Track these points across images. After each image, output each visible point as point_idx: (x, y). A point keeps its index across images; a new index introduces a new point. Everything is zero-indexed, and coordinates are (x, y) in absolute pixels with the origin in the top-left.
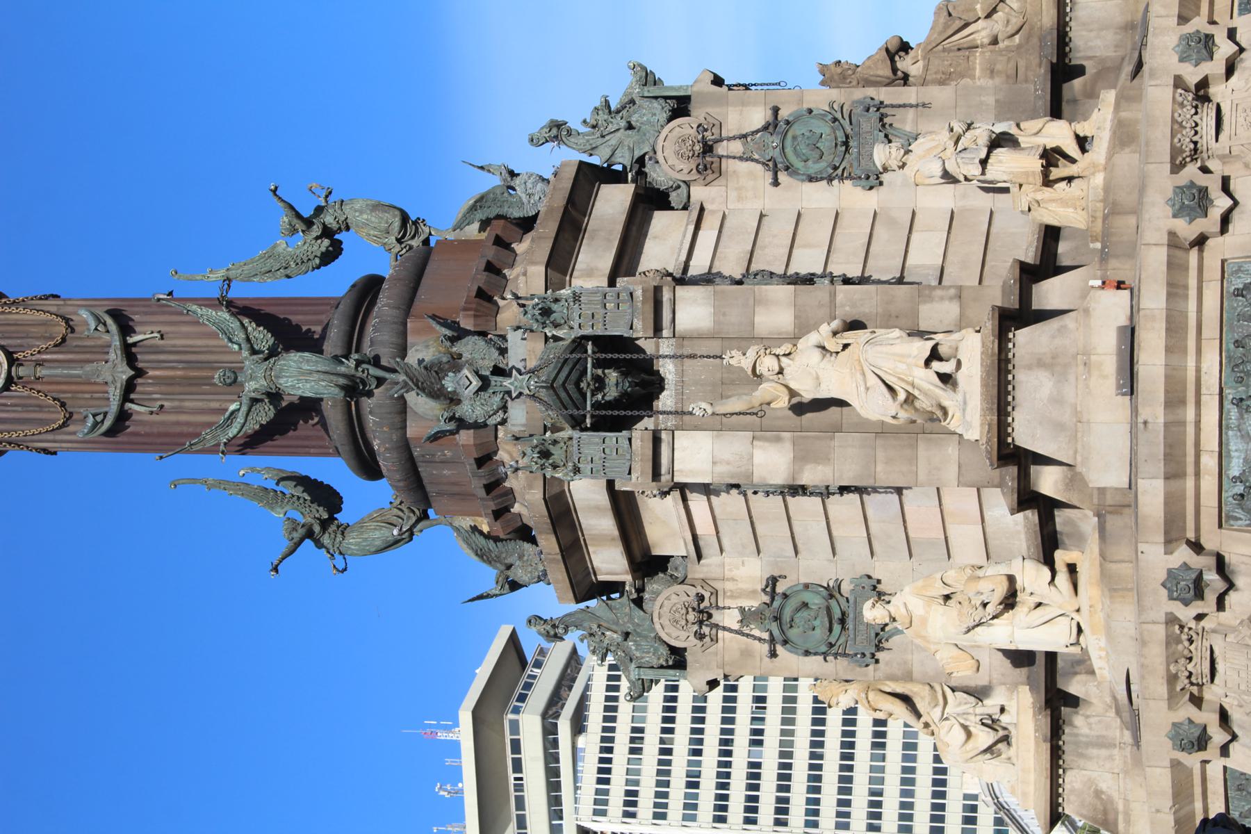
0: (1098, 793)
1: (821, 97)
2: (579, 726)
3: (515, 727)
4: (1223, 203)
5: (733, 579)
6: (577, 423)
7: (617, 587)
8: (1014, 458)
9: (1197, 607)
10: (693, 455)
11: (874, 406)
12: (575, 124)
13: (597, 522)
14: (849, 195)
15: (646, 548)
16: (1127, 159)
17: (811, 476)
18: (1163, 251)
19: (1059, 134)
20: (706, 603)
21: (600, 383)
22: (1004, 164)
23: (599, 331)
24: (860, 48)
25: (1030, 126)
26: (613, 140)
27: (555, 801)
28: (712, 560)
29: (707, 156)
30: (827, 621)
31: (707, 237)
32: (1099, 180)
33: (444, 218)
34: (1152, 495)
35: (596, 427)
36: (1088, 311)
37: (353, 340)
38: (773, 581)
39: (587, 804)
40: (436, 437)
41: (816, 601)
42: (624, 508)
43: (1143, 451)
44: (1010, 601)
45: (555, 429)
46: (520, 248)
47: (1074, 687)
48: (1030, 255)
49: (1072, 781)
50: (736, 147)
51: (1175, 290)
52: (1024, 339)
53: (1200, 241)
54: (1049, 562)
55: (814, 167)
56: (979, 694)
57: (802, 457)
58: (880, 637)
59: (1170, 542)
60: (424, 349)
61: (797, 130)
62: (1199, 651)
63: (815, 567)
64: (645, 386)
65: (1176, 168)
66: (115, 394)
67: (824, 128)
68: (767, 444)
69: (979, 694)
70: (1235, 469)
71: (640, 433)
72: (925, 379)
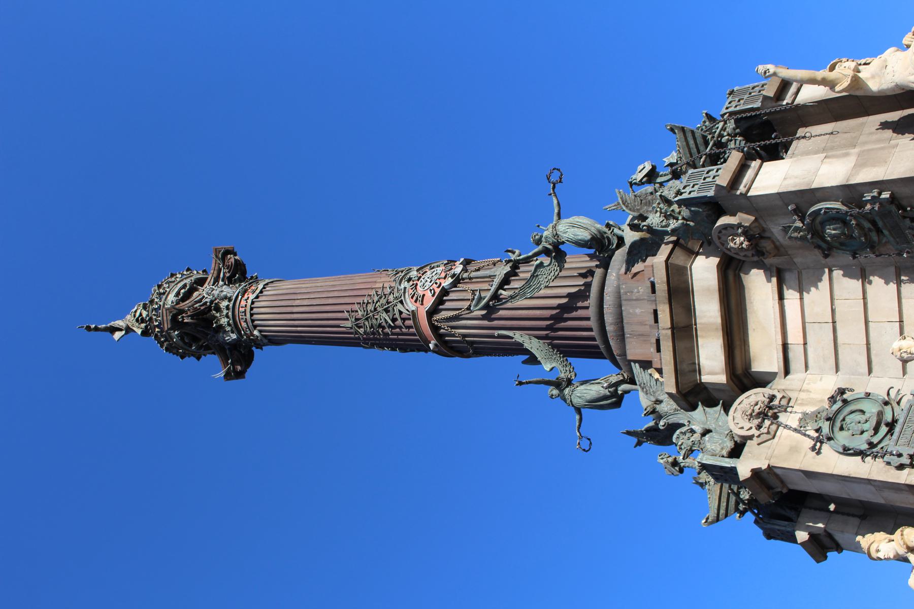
5: (808, 391)
15: (748, 364)
20: (776, 402)
41: (871, 409)
66: (497, 281)
68: (834, 160)
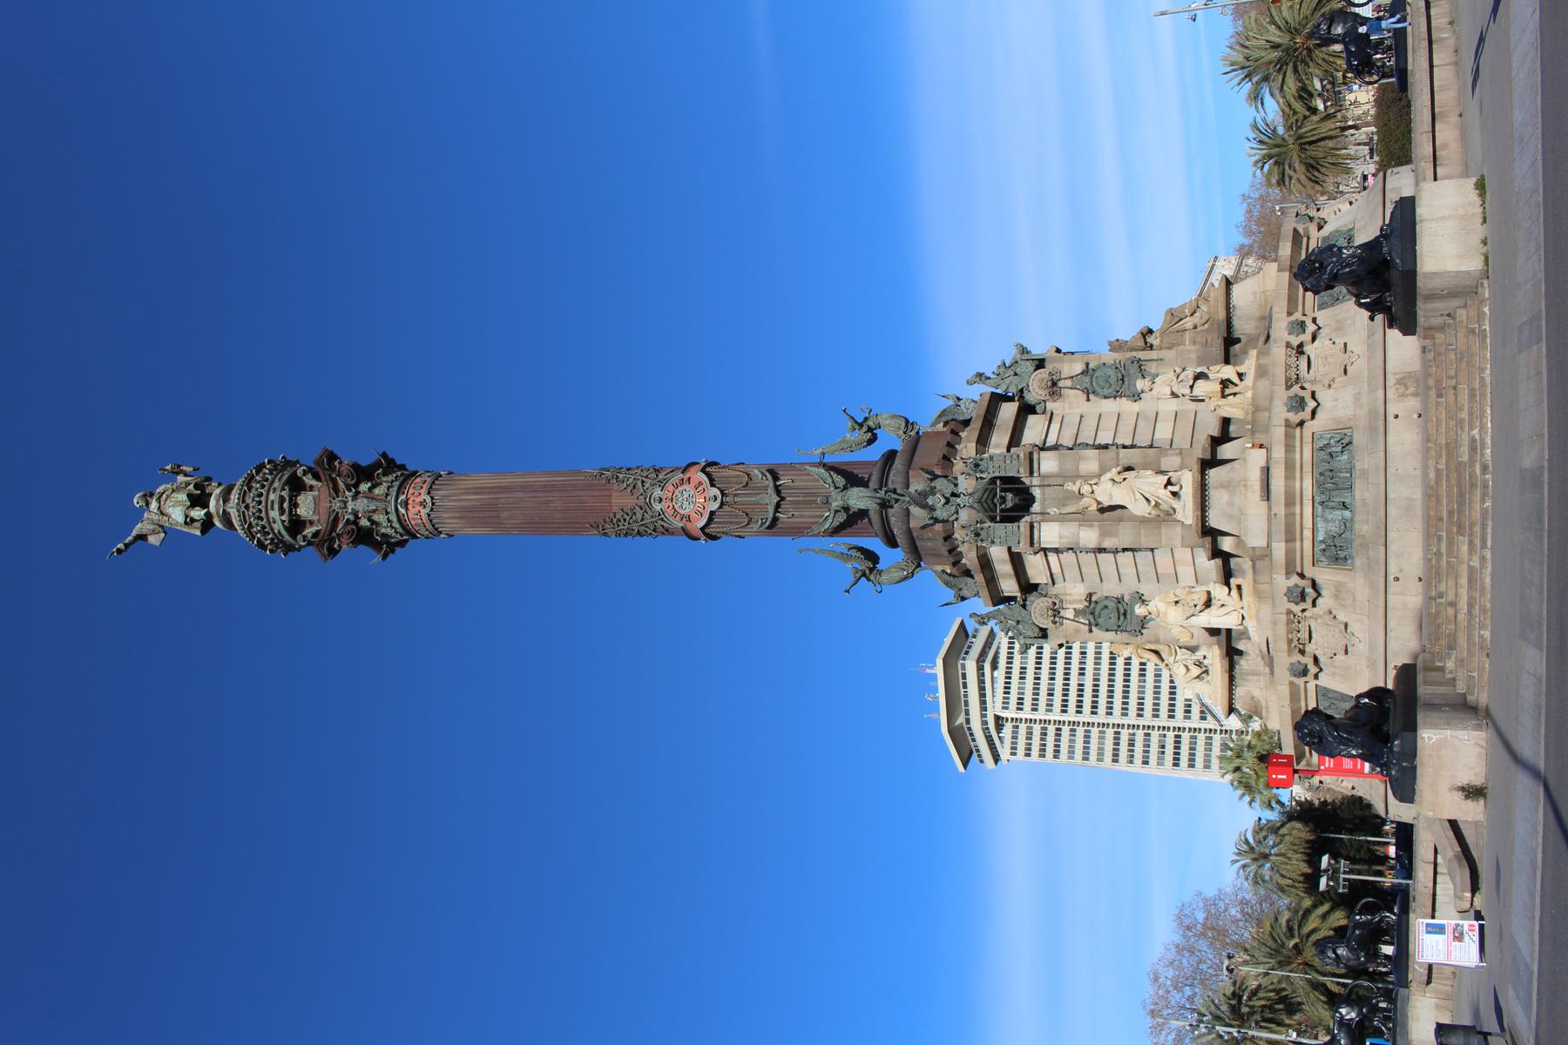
0: (1253, 698)
1: (1110, 357)
2: (994, 666)
3: (963, 666)
4: (1312, 404)
6: (993, 519)
7: (1013, 599)
8: (1210, 533)
9: (1302, 606)
10: (1050, 534)
11: (1139, 508)
12: (989, 374)
13: (1003, 567)
14: (1124, 405)
15: (1027, 580)
16: (1263, 384)
17: (1106, 545)
18: (1283, 429)
19: (1228, 372)
21: (1003, 500)
22: (1202, 388)
23: (1003, 474)
24: (1128, 332)
26: (1008, 381)
27: (983, 703)
28: (1060, 585)
29: (1054, 387)
30: (1116, 615)
31: (1055, 427)
32: (1249, 394)
33: (926, 421)
34: (1279, 550)
35: (1002, 521)
36: (1245, 459)
37: (883, 482)
38: (1090, 595)
39: (999, 704)
40: (924, 527)
41: (1111, 605)
42: (1016, 560)
43: (1274, 529)
44: (1208, 604)
45: (982, 522)
46: (963, 434)
47: (1240, 646)
48: (1215, 431)
49: (1239, 692)
50: (1068, 383)
51: (1289, 448)
52: (1214, 474)
53: (1301, 424)
54: (1227, 584)
55: (1107, 392)
56: (1193, 649)
57: (1104, 534)
58: (1143, 622)
59: (1288, 574)
60: (917, 485)
61: (1098, 374)
62: (1304, 627)
63: (1111, 588)
64: (1025, 500)
65: (1288, 387)
66: (771, 509)
67: (1111, 372)
69: (1193, 649)
71: (1024, 523)
72: (1165, 494)
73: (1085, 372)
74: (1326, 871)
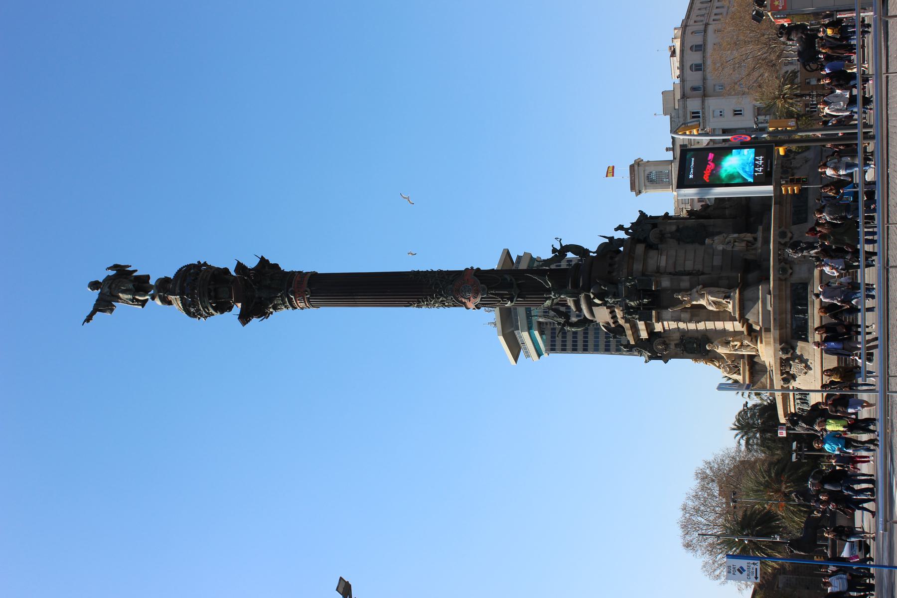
4: (790, 271)
19: (749, 237)
25: (742, 235)
29: (662, 238)
31: (664, 258)
46: (616, 259)
70: (794, 326)
73: (678, 230)
74: (795, 451)
